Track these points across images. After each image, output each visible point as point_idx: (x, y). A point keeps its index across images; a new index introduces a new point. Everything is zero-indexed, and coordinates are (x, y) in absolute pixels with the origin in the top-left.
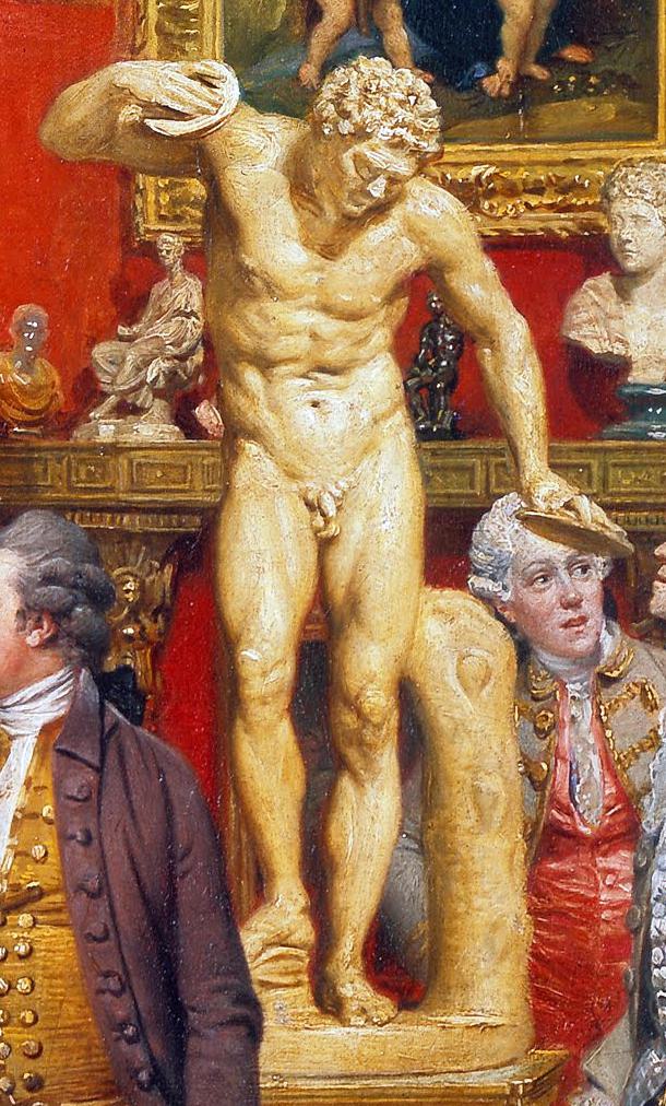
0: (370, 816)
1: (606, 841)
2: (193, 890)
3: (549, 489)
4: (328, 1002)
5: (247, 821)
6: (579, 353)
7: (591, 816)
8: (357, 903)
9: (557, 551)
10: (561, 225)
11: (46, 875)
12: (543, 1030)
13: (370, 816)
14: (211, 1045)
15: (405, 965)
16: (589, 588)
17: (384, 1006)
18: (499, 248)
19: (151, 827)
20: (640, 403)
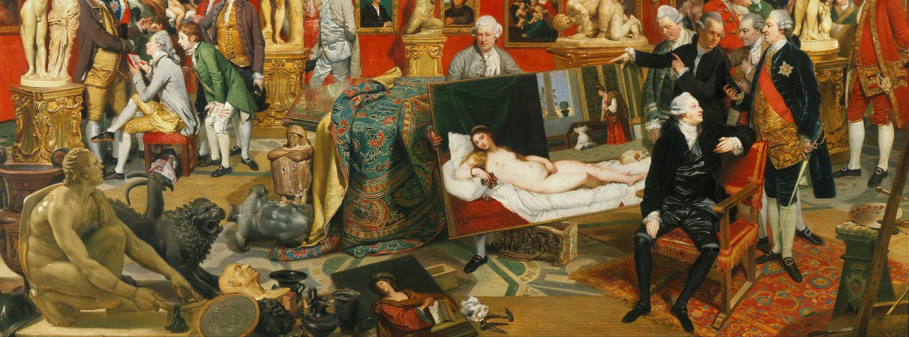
0: (281, 14)
1: (315, 18)
2: (255, 25)
4: (275, 41)
5: (263, 15)
7: (312, 14)
8: (279, 27)
11: (234, 23)
12: (305, 45)
13: (281, 14)
14: (258, 47)
15: (286, 36)
17: (283, 42)
19: (249, 16)
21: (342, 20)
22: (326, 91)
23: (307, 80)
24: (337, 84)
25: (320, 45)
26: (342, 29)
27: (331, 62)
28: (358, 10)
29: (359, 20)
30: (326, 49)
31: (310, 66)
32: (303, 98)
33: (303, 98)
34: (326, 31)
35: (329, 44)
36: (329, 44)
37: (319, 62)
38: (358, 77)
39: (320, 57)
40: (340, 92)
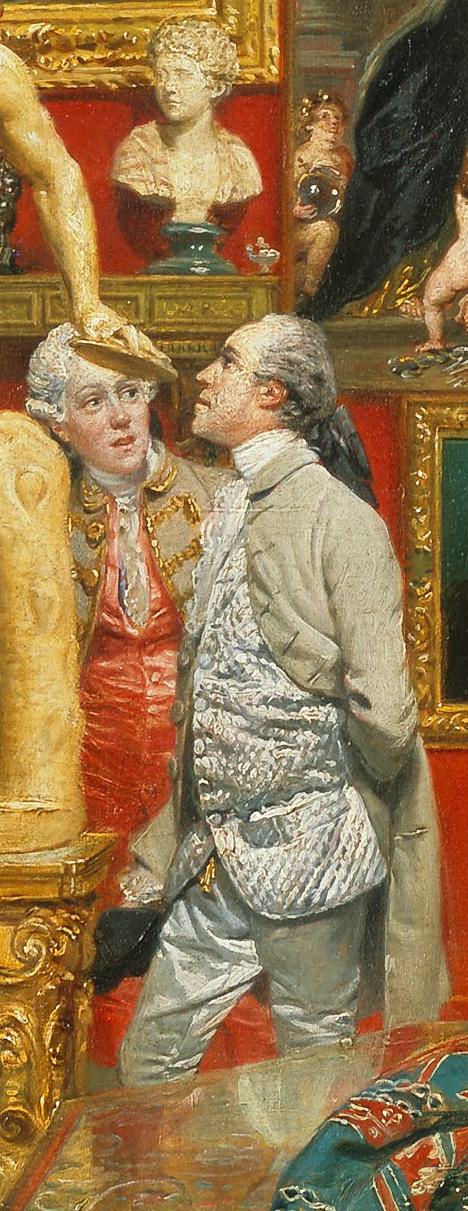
1: (152, 642)
3: (100, 320)
6: (127, 195)
7: (138, 619)
9: (107, 376)
10: (112, 77)
12: (94, 813)
16: (137, 410)
18: (55, 99)
20: (184, 240)
21: (330, 652)
22: (223, 1107)
23: (106, 1036)
24: (294, 1061)
25: (190, 816)
26: (329, 714)
27: (256, 924)
28: (431, 590)
29: (433, 657)
30: (226, 837)
31: (124, 949)
32: (78, 1149)
33: (78, 1149)
34: (228, 726)
35: (242, 807)
36: (242, 807)
37: (179, 924)
38: (430, 1017)
39: (187, 889)
40: (315, 1109)
